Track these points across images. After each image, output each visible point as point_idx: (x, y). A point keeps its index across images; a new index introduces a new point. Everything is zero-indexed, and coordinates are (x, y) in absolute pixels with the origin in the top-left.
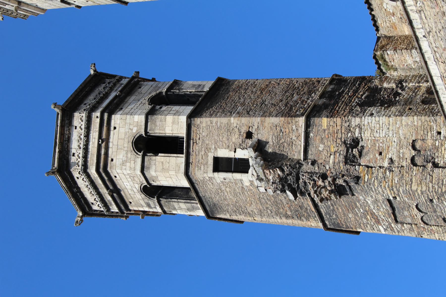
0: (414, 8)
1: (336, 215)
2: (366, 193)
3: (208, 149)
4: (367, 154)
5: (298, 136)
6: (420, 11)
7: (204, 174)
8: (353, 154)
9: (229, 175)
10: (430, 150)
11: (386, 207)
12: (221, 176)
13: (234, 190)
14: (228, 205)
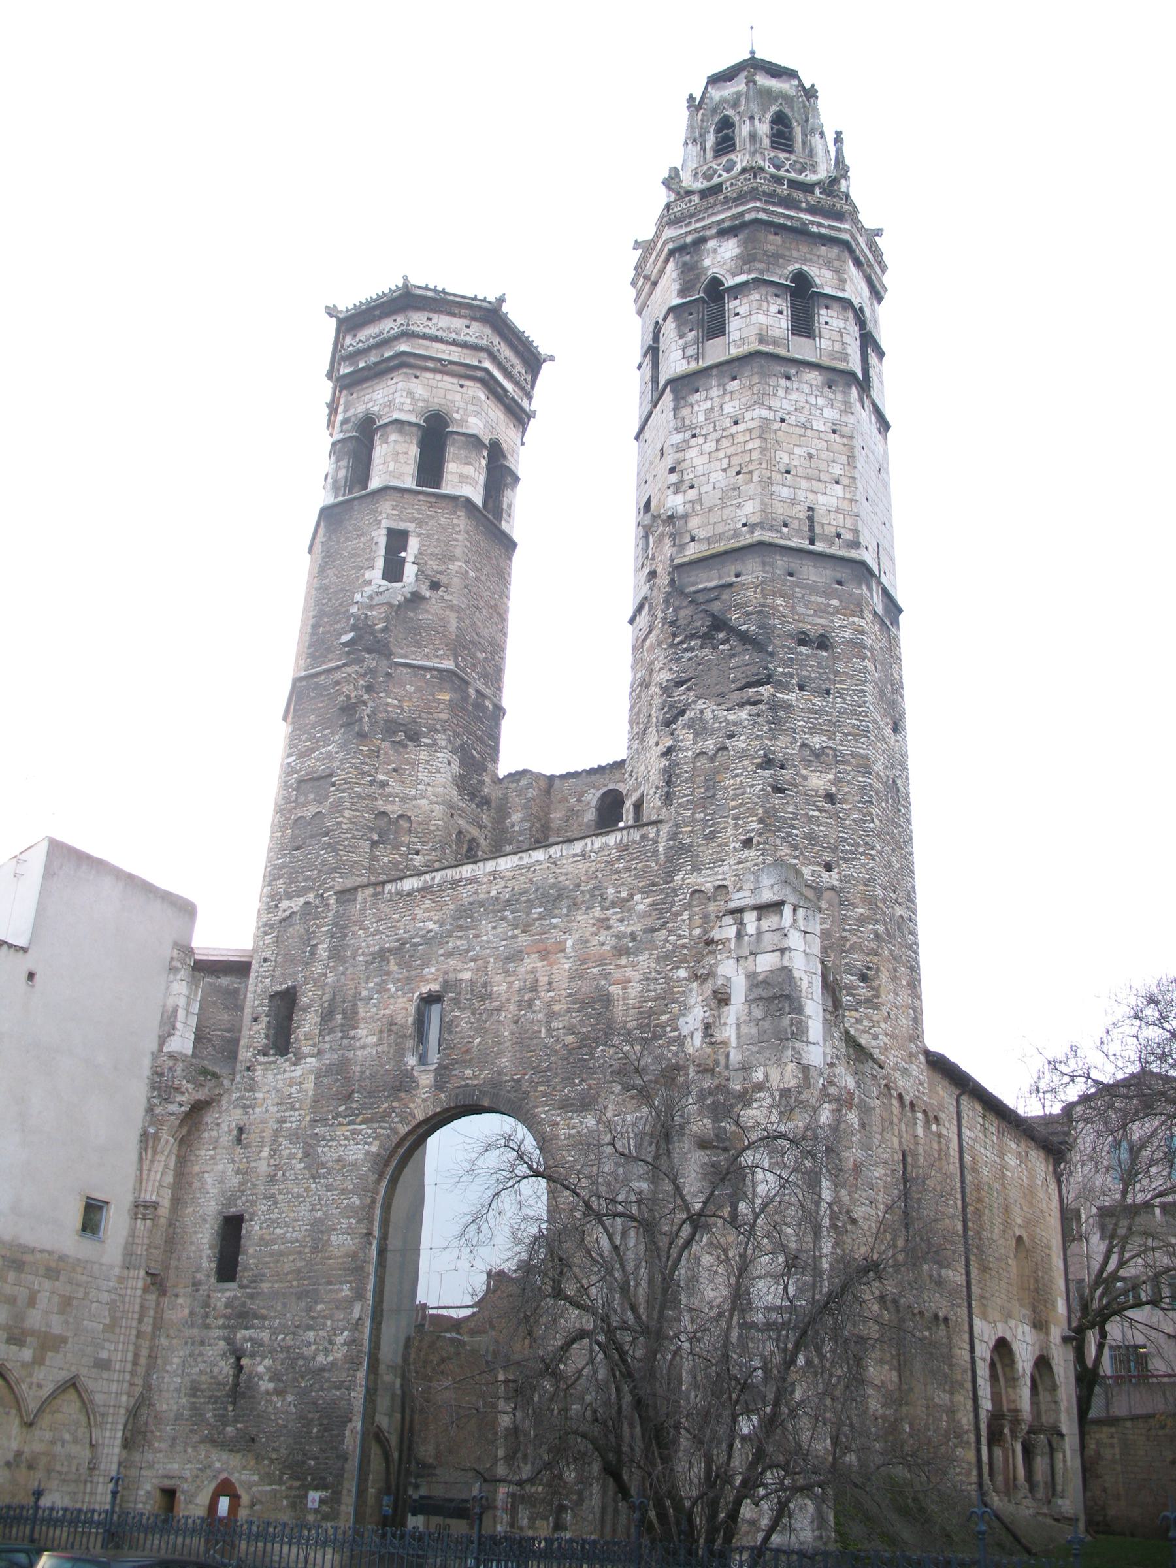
2: (343, 746)
7: (387, 516)
9: (382, 552)
11: (321, 768)
12: (383, 542)
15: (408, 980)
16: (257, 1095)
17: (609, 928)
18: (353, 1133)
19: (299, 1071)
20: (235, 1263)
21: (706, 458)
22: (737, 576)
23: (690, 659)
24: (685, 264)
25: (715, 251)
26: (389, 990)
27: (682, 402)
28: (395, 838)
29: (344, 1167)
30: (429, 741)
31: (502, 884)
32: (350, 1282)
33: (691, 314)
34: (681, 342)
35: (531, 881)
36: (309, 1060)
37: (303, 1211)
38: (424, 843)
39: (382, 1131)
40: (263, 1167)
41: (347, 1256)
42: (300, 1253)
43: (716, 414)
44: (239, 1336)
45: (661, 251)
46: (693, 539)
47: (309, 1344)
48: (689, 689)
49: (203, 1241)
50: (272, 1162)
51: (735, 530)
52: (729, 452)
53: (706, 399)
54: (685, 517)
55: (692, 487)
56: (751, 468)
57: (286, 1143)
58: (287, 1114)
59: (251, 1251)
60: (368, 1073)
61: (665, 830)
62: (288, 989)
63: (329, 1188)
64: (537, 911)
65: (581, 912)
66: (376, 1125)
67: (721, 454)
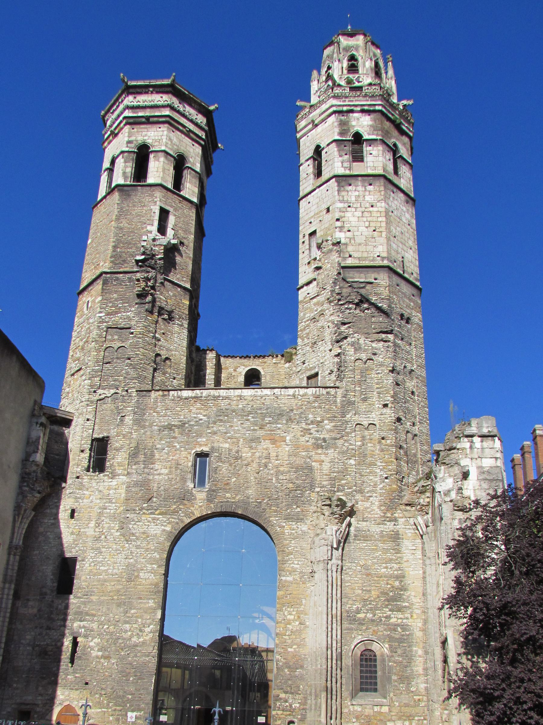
0: (297, 393)
1: (116, 285)
4: (164, 324)
5: (178, 279)
6: (294, 396)
8: (164, 314)
13: (143, 217)
14: (128, 206)
16: (85, 492)
17: (311, 434)
18: (154, 519)
19: (114, 483)
21: (356, 219)
22: (375, 279)
23: (350, 313)
24: (341, 120)
25: (358, 119)
26: (175, 446)
27: (342, 189)
29: (148, 537)
30: (180, 323)
31: (246, 402)
32: (154, 599)
33: (345, 146)
34: (340, 159)
35: (263, 404)
36: (121, 477)
37: (120, 558)
39: (173, 520)
40: (90, 532)
41: (151, 584)
42: (119, 581)
43: (361, 199)
45: (327, 110)
46: (350, 256)
47: (126, 631)
48: (349, 327)
51: (374, 257)
52: (369, 219)
53: (355, 190)
54: (346, 244)
55: (349, 231)
57: (107, 520)
58: (106, 505)
59: (83, 578)
60: (162, 488)
61: (340, 392)
62: (104, 437)
63: (138, 547)
64: (267, 419)
65: (294, 424)
67: (365, 219)
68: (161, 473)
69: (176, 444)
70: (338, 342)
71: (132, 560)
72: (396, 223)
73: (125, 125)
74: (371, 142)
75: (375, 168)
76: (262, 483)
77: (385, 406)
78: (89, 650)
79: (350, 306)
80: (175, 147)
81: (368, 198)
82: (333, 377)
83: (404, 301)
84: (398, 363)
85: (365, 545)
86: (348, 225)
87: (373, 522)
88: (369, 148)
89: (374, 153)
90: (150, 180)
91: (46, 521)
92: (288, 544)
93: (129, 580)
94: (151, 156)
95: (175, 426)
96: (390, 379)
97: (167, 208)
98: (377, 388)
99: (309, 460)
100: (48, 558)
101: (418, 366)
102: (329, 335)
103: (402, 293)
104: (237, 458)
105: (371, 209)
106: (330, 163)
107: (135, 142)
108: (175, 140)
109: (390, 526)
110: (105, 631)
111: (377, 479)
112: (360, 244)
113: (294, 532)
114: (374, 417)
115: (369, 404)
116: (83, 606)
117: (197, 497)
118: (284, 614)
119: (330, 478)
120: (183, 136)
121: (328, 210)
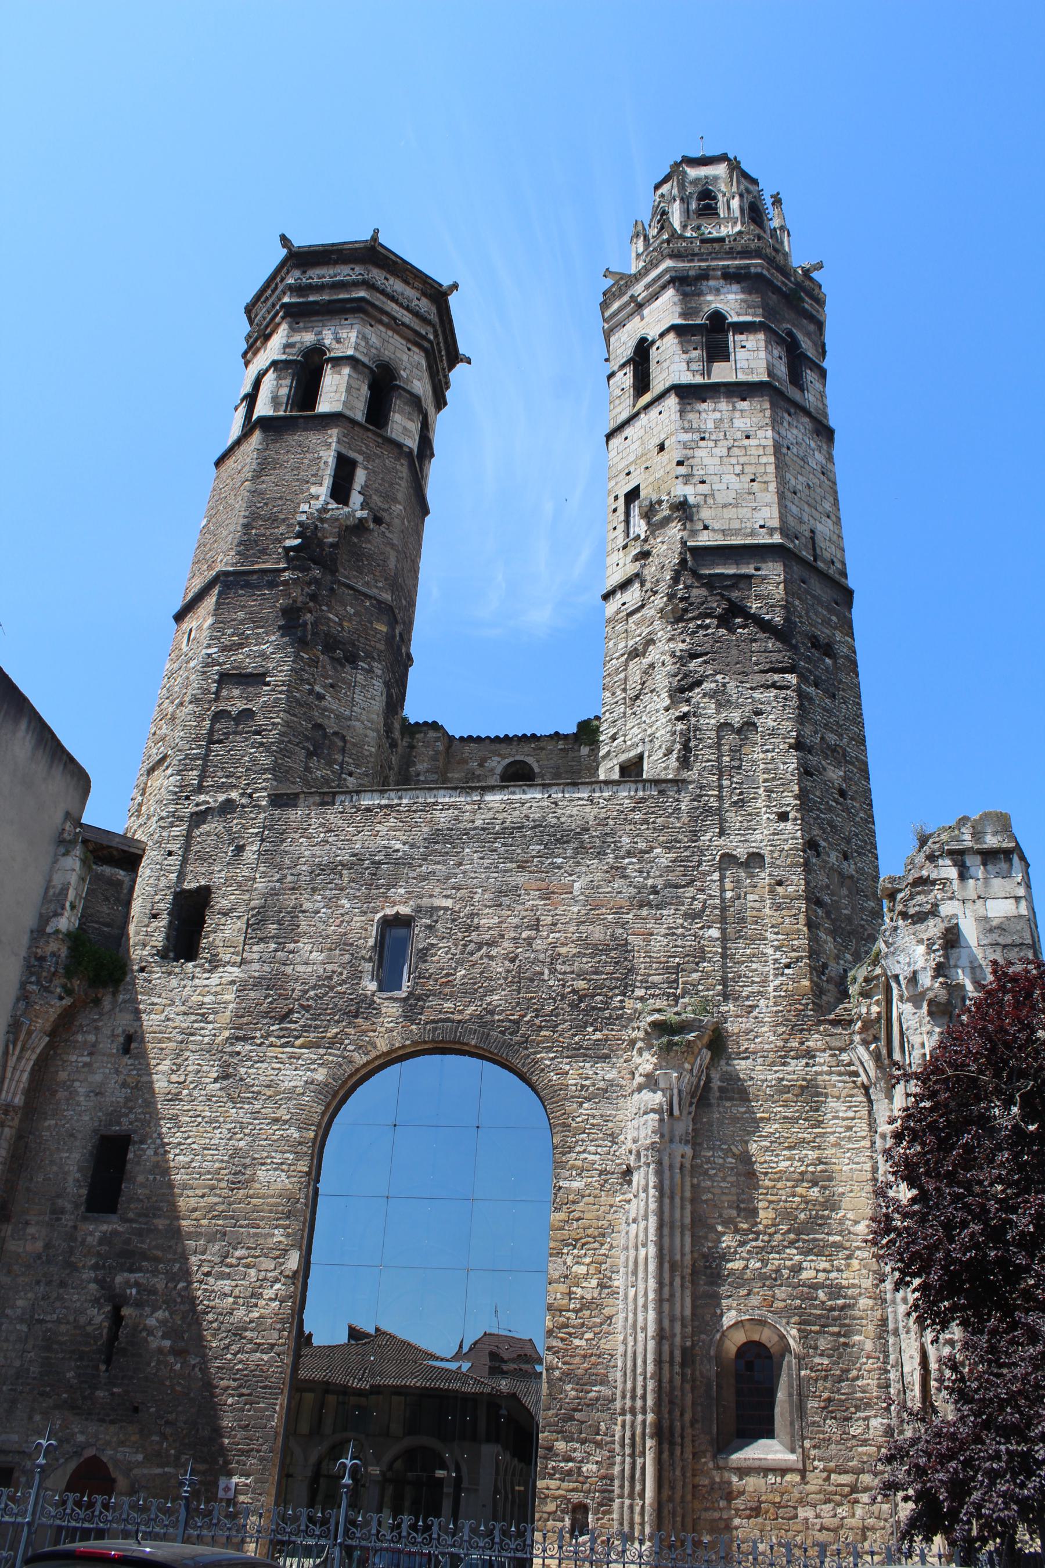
3: (368, 458)
4: (335, 668)
10: (329, 754)
15: (368, 898)
17: (625, 877)
20: (117, 1192)
21: (717, 461)
22: (757, 569)
27: (689, 408)
28: (329, 754)
31: (490, 814)
34: (684, 356)
35: (527, 817)
36: (229, 968)
37: (218, 1136)
38: (357, 766)
39: (331, 1058)
44: (119, 1279)
46: (706, 528)
48: (706, 662)
49: (69, 1164)
50: (174, 1078)
52: (742, 460)
54: (698, 506)
55: (703, 482)
56: (766, 479)
58: (196, 1025)
59: (140, 1178)
62: (199, 888)
66: (322, 1051)
67: (734, 461)
68: (310, 959)
69: (344, 901)
70: (682, 690)
71: (242, 1143)
72: (797, 468)
73: (283, 318)
74: (742, 328)
75: (752, 371)
76: (522, 979)
77: (783, 817)
78: (144, 1334)
79: (708, 621)
80: (374, 351)
81: (738, 423)
82: (673, 762)
83: (816, 613)
84: (808, 730)
85: (743, 1110)
86: (702, 472)
87: (760, 1060)
88: (738, 337)
89: (749, 345)
90: (324, 406)
91: (73, 1058)
92: (575, 1111)
93: (235, 1185)
94: (328, 369)
95: (341, 863)
96: (790, 764)
97: (352, 455)
98: (765, 781)
99: (621, 931)
100: (72, 1135)
101: (852, 739)
102: (661, 680)
103: (814, 597)
104: (469, 929)
105: (746, 442)
106: (665, 365)
107: (298, 345)
108: (374, 339)
109: (797, 1066)
110: (179, 1294)
111: (770, 968)
112: (725, 506)
113: (587, 1083)
114: (760, 839)
115: (750, 815)
116: (135, 1240)
117: (384, 1010)
118: (565, 1263)
119: (668, 968)
120: (390, 333)
121: (662, 448)
